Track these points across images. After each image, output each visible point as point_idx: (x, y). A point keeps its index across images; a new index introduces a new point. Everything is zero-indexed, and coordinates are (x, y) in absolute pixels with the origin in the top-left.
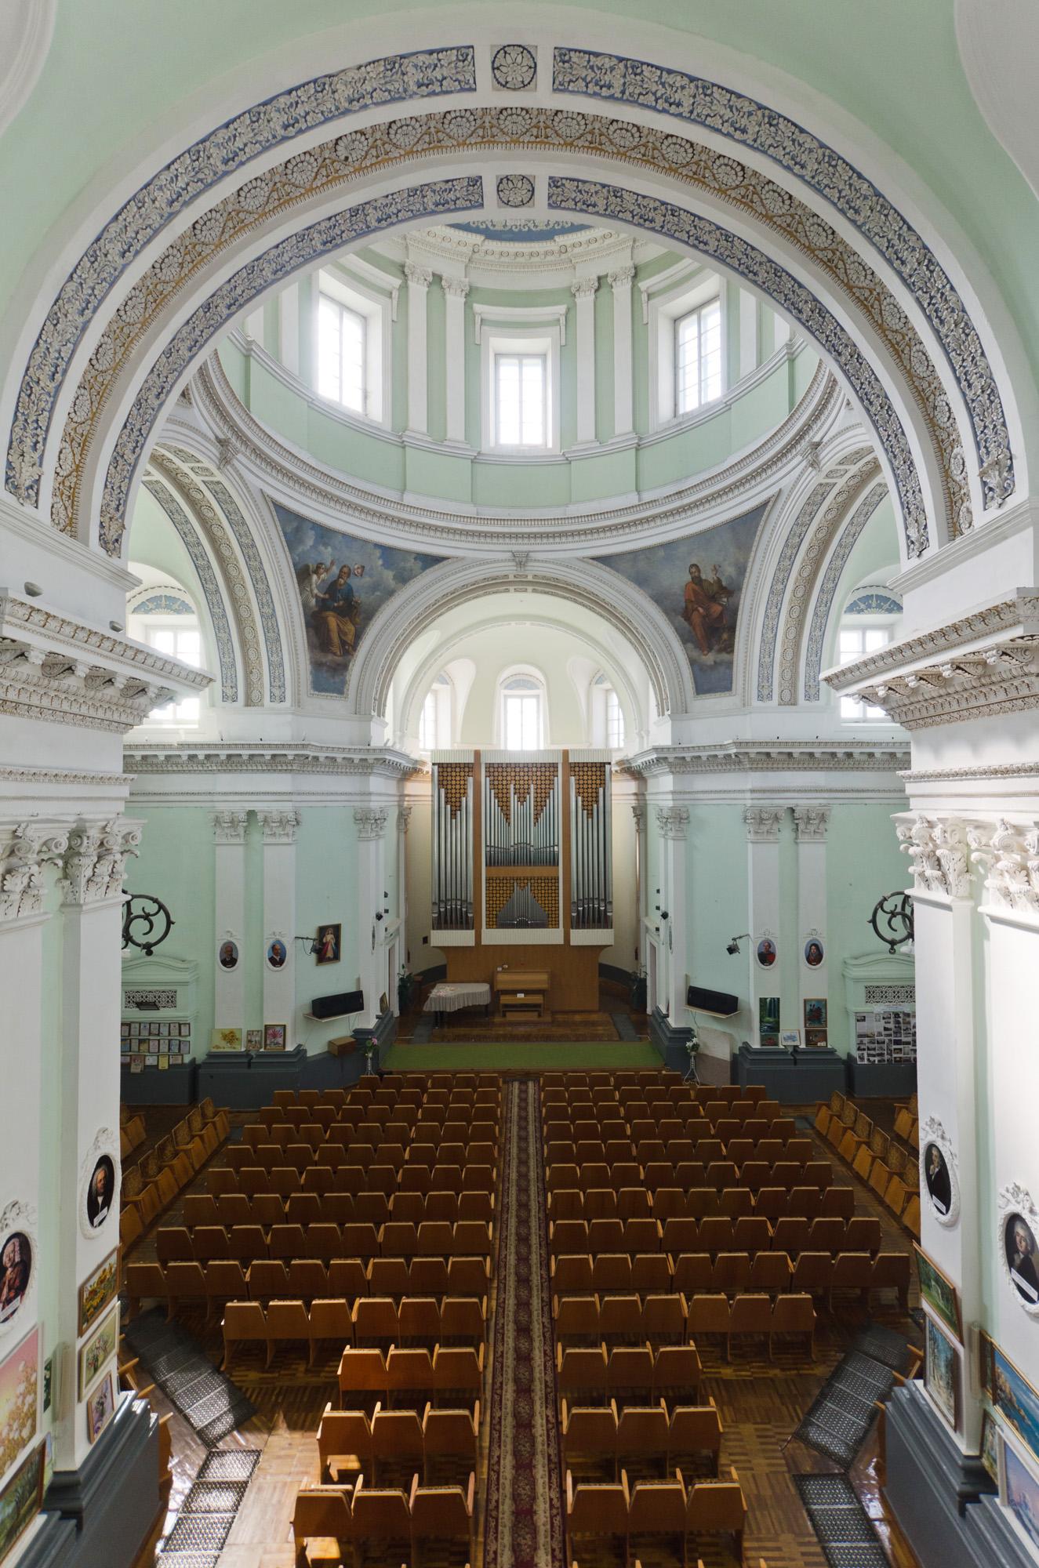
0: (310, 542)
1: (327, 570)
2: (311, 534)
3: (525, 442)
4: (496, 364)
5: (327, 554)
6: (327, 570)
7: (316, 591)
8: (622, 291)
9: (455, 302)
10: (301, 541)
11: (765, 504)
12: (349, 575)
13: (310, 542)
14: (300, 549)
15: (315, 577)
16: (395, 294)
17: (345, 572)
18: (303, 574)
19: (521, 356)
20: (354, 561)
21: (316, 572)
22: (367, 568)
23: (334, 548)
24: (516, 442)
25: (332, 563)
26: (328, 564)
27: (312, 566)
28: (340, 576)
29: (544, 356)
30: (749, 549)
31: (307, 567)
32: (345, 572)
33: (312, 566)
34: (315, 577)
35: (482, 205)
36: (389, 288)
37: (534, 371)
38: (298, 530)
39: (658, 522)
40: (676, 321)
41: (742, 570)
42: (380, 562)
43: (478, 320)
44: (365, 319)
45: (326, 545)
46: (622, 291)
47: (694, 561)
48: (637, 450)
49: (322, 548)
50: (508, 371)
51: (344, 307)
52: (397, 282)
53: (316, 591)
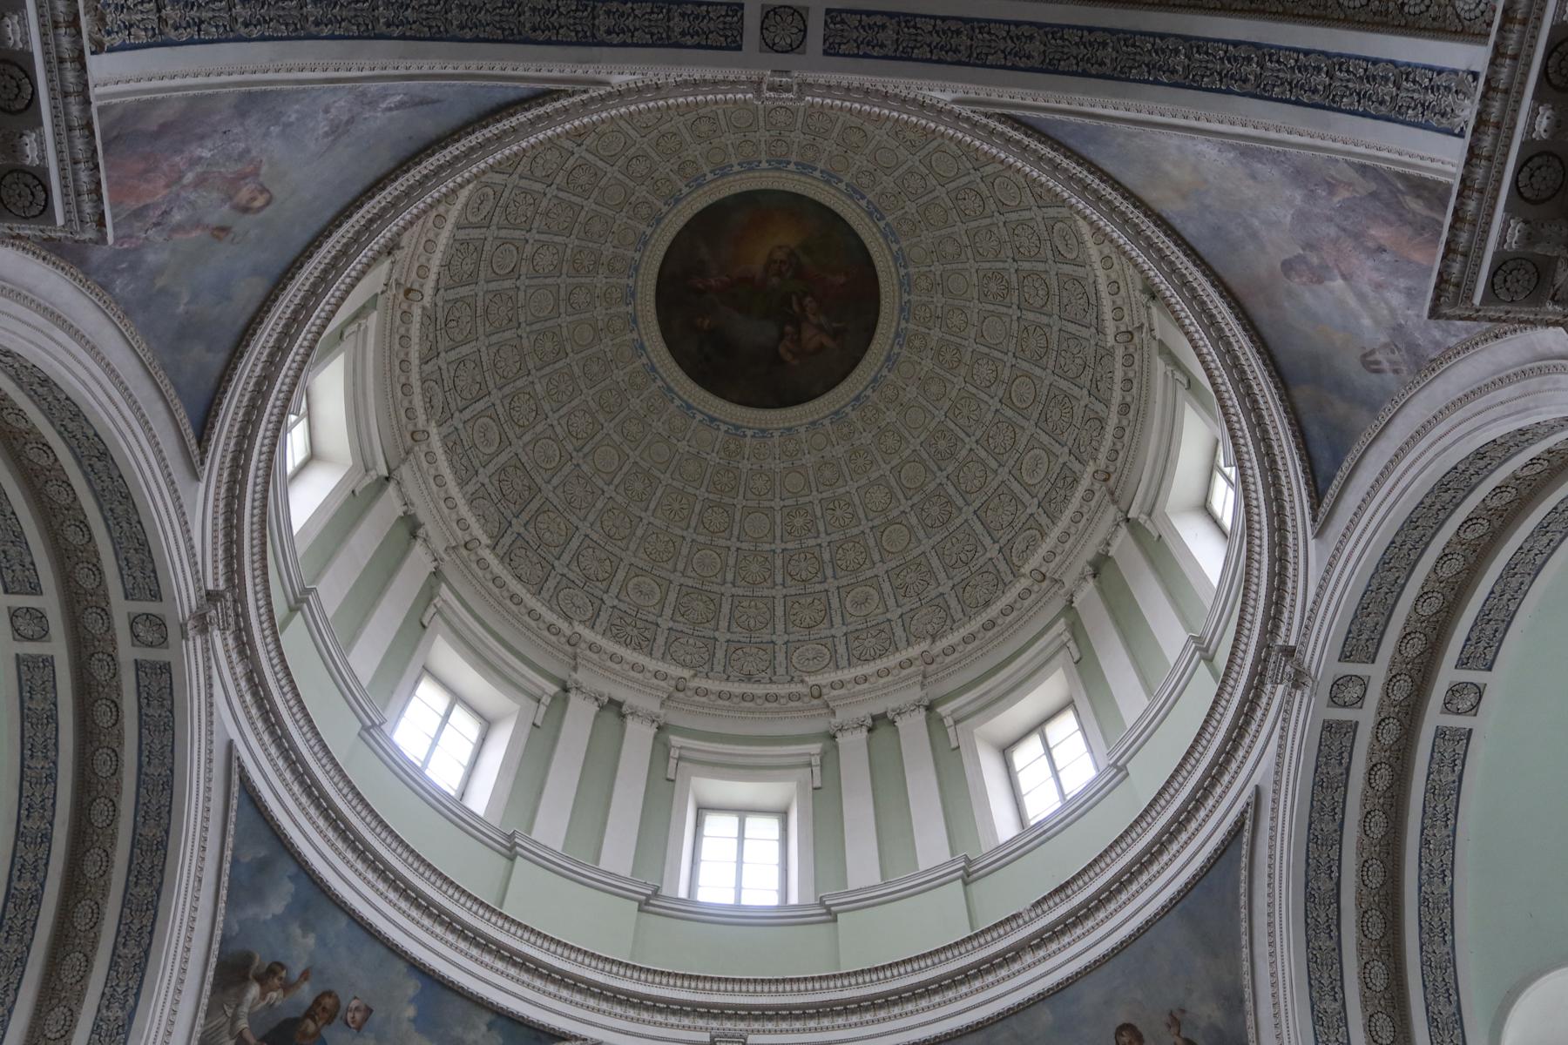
0: (277, 905)
1: (287, 987)
2: (288, 887)
3: (747, 900)
4: (699, 824)
5: (301, 949)
6: (287, 987)
7: (243, 1024)
8: (913, 727)
9: (639, 736)
10: (258, 895)
11: (1238, 827)
12: (329, 1022)
13: (277, 905)
14: (251, 911)
15: (254, 990)
16: (546, 700)
17: (325, 1008)
18: (233, 971)
19: (743, 811)
20: (356, 981)
21: (262, 979)
22: (377, 1017)
23: (322, 941)
24: (730, 900)
25: (305, 975)
26: (296, 972)
27: (261, 960)
28: (310, 1014)
29: (783, 815)
30: (1235, 947)
31: (248, 958)
32: (325, 1008)
33: (261, 960)
34: (254, 990)
35: (739, 48)
36: (538, 692)
37: (764, 830)
38: (263, 866)
39: (1028, 958)
40: (1006, 751)
41: (1234, 1000)
42: (410, 1012)
43: (674, 753)
44: (488, 725)
45: (307, 927)
46: (913, 727)
47: (1122, 1019)
48: (966, 884)
49: (296, 930)
50: (719, 827)
51: (457, 698)
52: (553, 689)
53: (243, 1024)
